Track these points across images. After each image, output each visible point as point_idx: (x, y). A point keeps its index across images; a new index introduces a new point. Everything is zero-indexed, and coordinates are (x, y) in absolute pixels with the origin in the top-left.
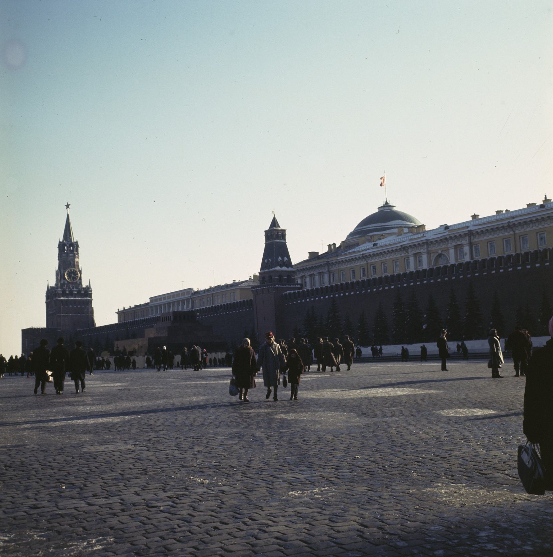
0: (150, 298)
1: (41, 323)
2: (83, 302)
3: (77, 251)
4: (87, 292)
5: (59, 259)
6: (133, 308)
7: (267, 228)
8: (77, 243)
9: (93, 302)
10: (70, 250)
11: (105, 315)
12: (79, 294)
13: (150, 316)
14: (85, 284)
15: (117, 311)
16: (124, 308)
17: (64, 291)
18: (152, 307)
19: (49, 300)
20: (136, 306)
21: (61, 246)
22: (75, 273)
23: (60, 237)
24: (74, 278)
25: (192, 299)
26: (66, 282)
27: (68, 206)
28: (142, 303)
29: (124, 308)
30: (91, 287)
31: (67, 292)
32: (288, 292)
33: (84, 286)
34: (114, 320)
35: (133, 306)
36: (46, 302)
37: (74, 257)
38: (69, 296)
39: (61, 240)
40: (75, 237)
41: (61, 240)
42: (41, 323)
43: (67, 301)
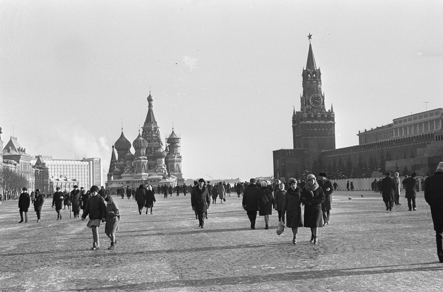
0: (394, 120)
1: (289, 145)
2: (327, 125)
3: (320, 78)
4: (330, 116)
6: (375, 130)
8: (319, 70)
11: (345, 137)
12: (323, 118)
13: (394, 137)
15: (358, 133)
16: (366, 130)
17: (309, 115)
18: (396, 129)
20: (378, 128)
21: (305, 74)
22: (318, 98)
24: (318, 104)
25: (441, 119)
26: (311, 107)
27: (310, 37)
28: (385, 124)
29: (366, 130)
30: (334, 111)
31: (312, 116)
33: (327, 111)
34: (356, 142)
35: (375, 127)
37: (317, 83)
38: (312, 120)
39: (305, 69)
40: (318, 65)
41: (305, 69)
42: (289, 145)
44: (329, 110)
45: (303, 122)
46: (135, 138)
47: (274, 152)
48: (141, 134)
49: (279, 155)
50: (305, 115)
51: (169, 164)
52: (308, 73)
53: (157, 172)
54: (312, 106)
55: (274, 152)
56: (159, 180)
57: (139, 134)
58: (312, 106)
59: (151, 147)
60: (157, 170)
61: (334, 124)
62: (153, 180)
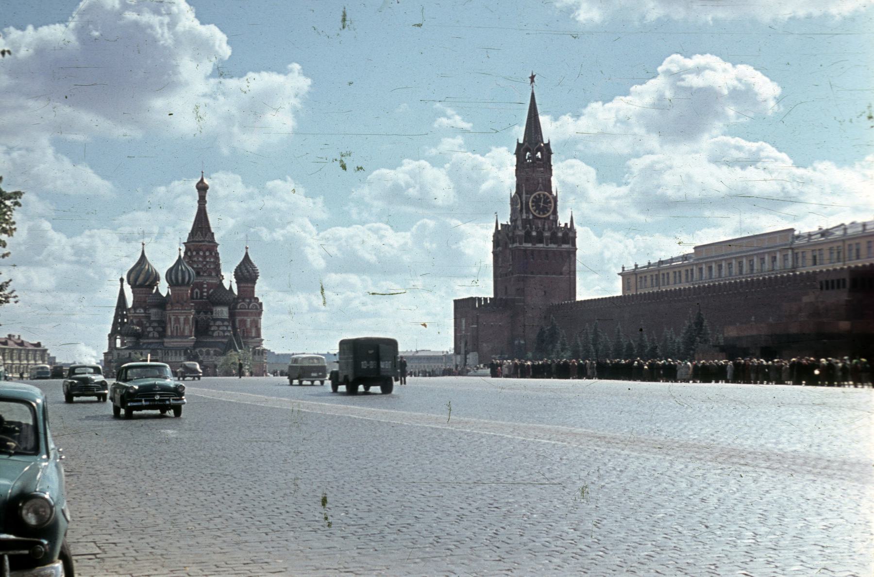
0: (695, 248)
1: (485, 289)
4: (569, 236)
5: (516, 175)
10: (538, 159)
12: (554, 239)
14: (563, 220)
15: (621, 271)
16: (636, 265)
20: (661, 262)
21: (520, 151)
23: (519, 133)
26: (531, 217)
29: (636, 265)
30: (576, 226)
36: (494, 252)
39: (521, 141)
41: (521, 141)
42: (485, 289)
44: (566, 224)
45: (516, 245)
46: (171, 264)
47: (455, 301)
48: (182, 255)
49: (463, 307)
50: (521, 232)
51: (238, 318)
52: (528, 150)
54: (534, 215)
57: (180, 256)
58: (534, 215)
59: (202, 284)
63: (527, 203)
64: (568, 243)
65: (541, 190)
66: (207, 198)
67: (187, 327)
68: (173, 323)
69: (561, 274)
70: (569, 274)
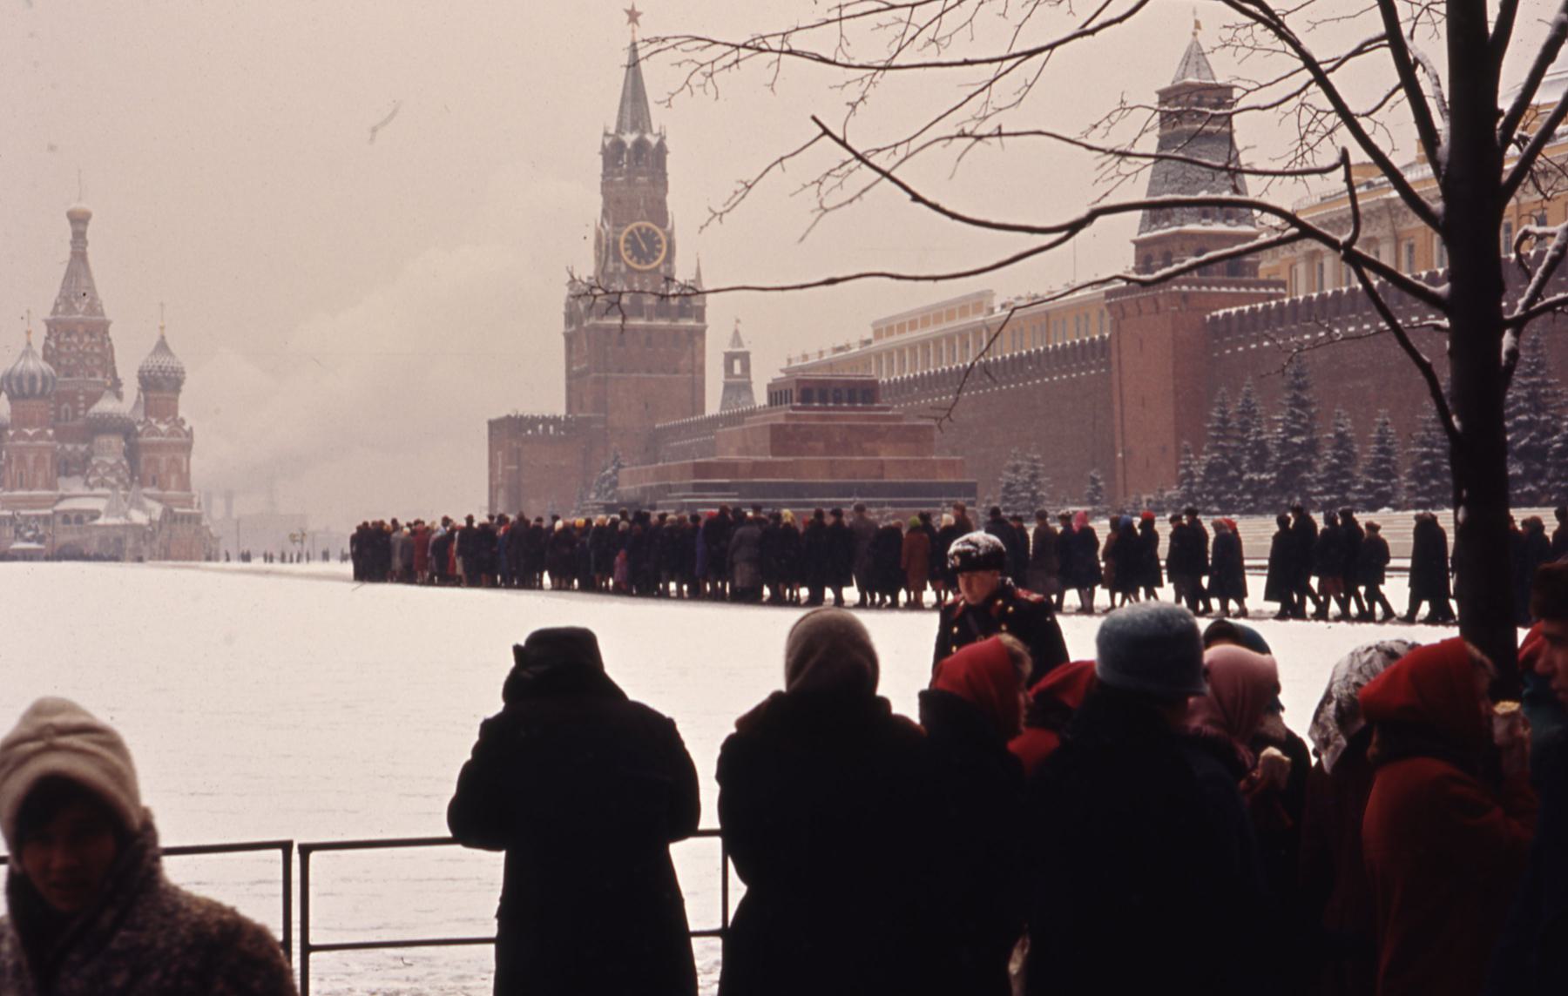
0: (875, 324)
2: (676, 333)
7: (1166, 84)
9: (708, 332)
19: (574, 328)
21: (613, 153)
26: (623, 269)
32: (1221, 313)
41: (612, 131)
43: (648, 330)
45: (592, 320)
47: (494, 426)
49: (510, 434)
51: (144, 457)
53: (92, 487)
54: (628, 266)
55: (494, 426)
56: (95, 515)
60: (91, 480)
61: (701, 333)
62: (73, 516)
63: (616, 243)
64: (689, 316)
65: (642, 219)
66: (89, 237)
67: (40, 474)
68: (13, 467)
69: (676, 372)
70: (693, 372)
